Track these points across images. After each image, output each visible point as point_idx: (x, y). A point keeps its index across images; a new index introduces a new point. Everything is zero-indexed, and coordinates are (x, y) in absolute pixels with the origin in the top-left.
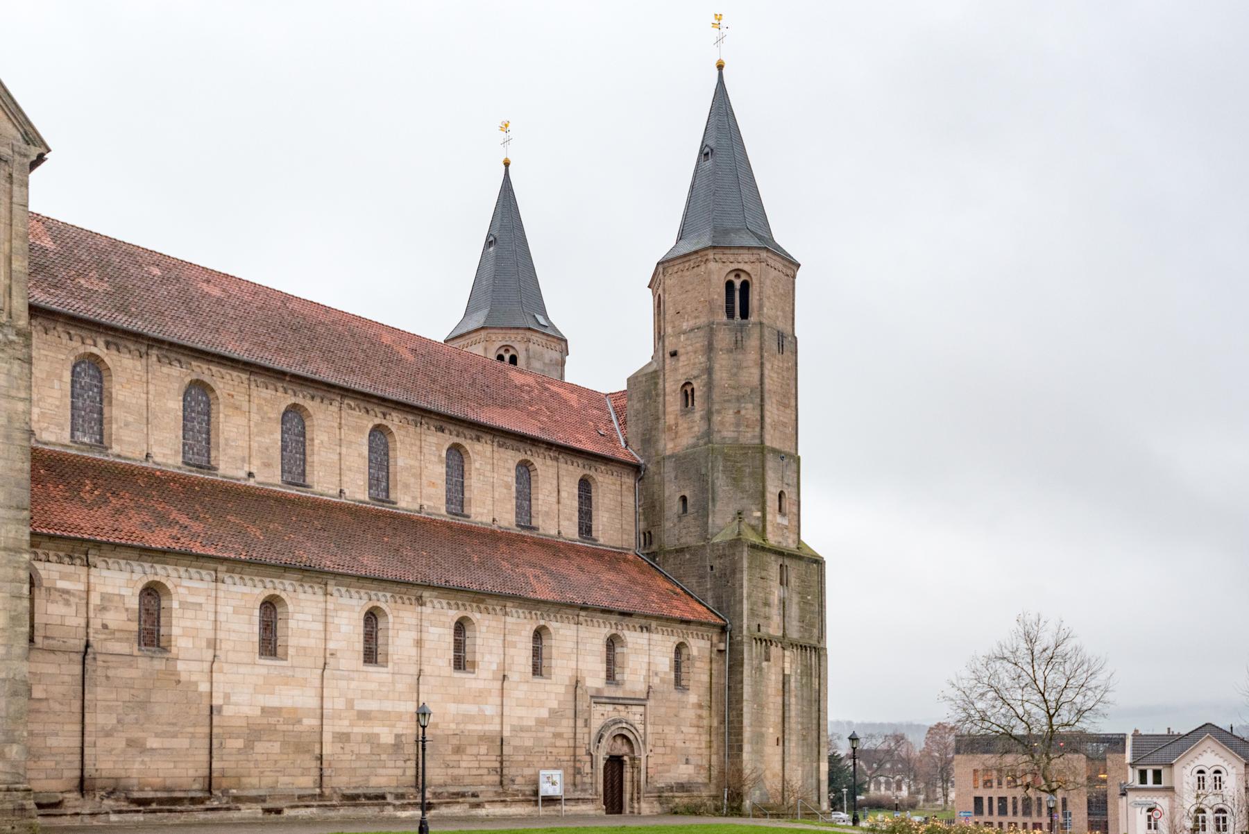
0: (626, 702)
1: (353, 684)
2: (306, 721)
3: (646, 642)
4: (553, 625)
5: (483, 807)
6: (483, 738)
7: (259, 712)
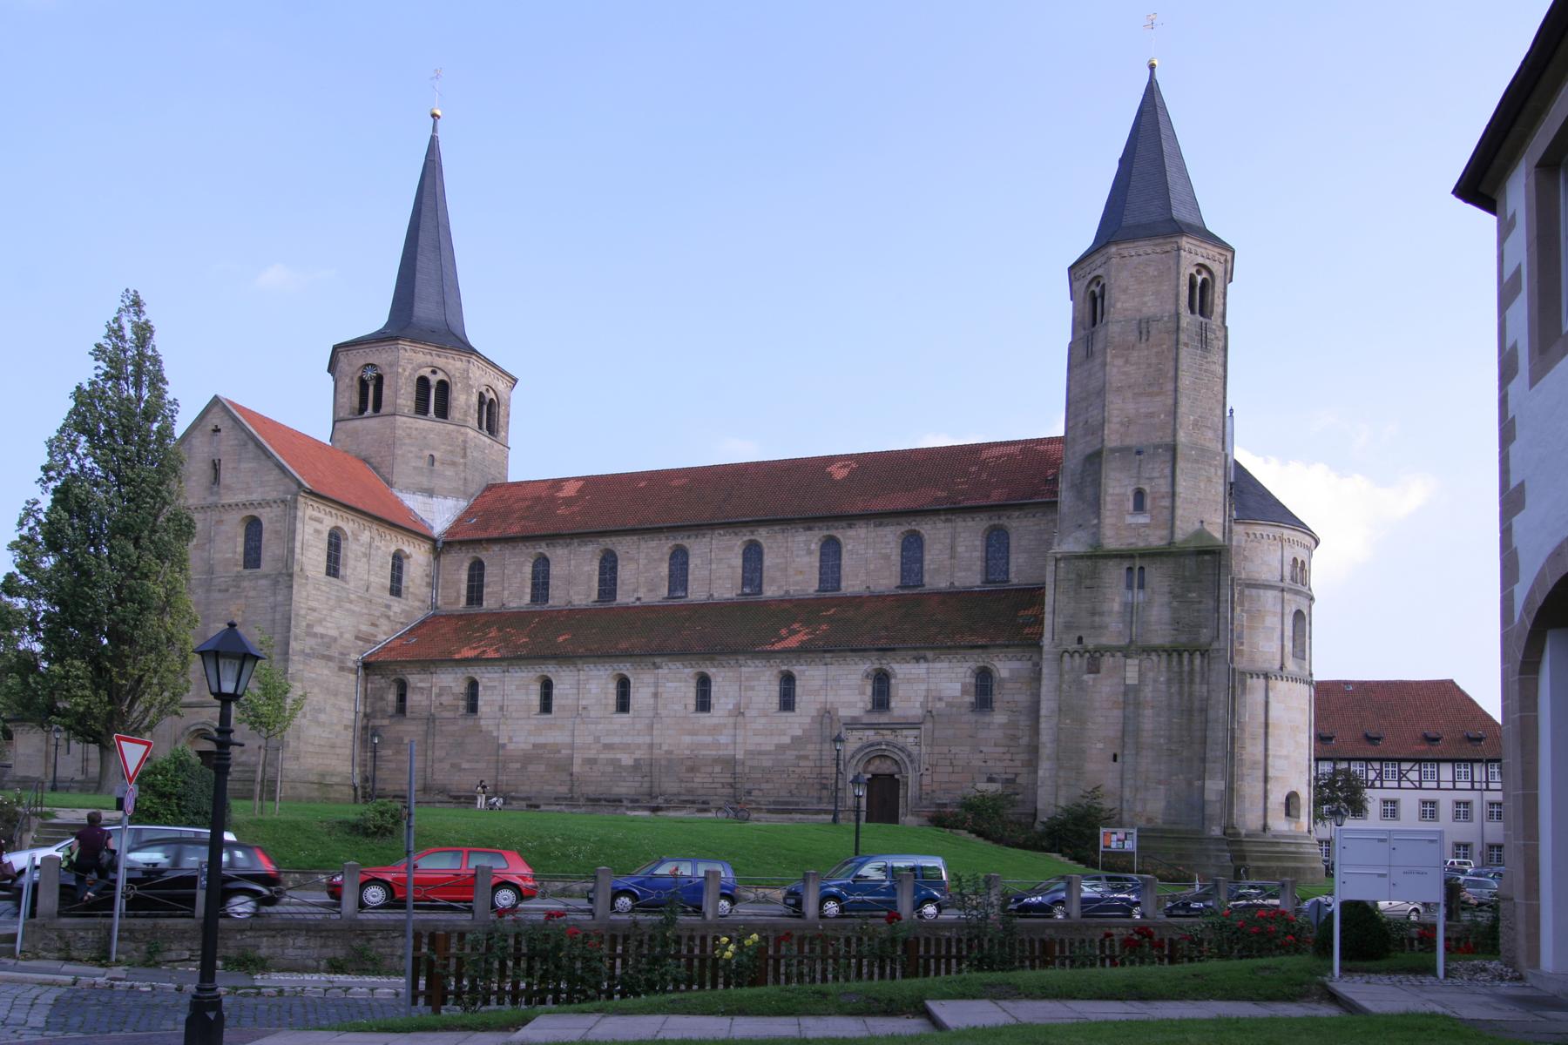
0: (894, 727)
1: (600, 727)
2: (563, 751)
3: (924, 671)
4: (796, 670)
6: (717, 760)
7: (531, 747)
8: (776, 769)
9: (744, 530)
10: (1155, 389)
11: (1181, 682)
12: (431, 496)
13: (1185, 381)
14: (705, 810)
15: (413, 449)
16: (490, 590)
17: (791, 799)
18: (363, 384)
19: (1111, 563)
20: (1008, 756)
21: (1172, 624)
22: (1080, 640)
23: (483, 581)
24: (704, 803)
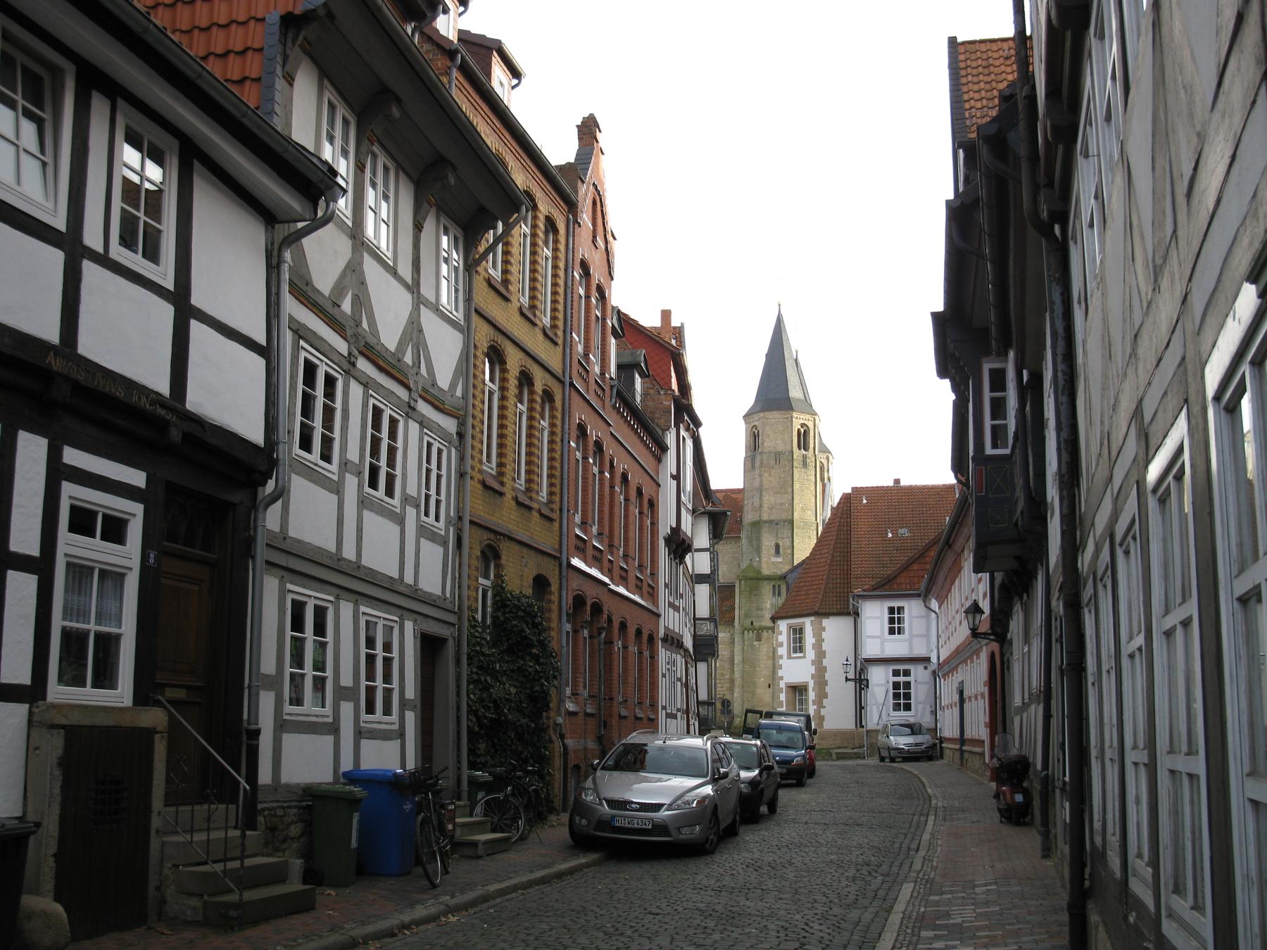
13: (797, 486)
22: (752, 623)
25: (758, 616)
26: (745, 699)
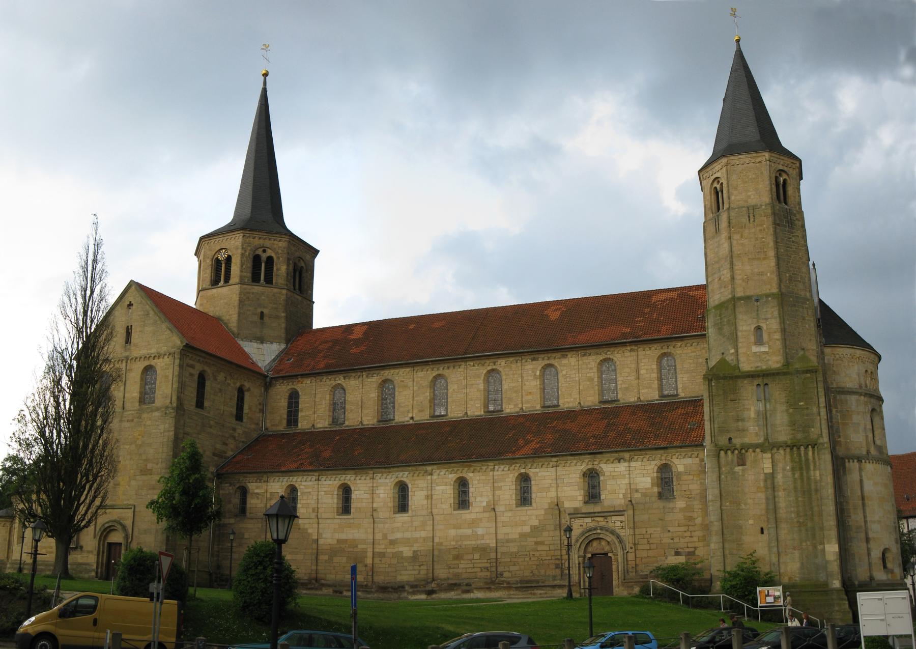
0: (606, 514)
1: (387, 526)
2: (360, 546)
3: (623, 469)
4: (532, 472)
5: (473, 592)
6: (476, 549)
8: (520, 553)
9: (488, 362)
10: (762, 256)
11: (801, 469)
12: (262, 343)
14: (468, 592)
15: (250, 308)
16: (303, 414)
17: (533, 578)
18: (218, 262)
19: (746, 382)
20: (688, 534)
21: (790, 426)
23: (298, 407)
24: (467, 585)
25: (739, 430)
26: (727, 552)
